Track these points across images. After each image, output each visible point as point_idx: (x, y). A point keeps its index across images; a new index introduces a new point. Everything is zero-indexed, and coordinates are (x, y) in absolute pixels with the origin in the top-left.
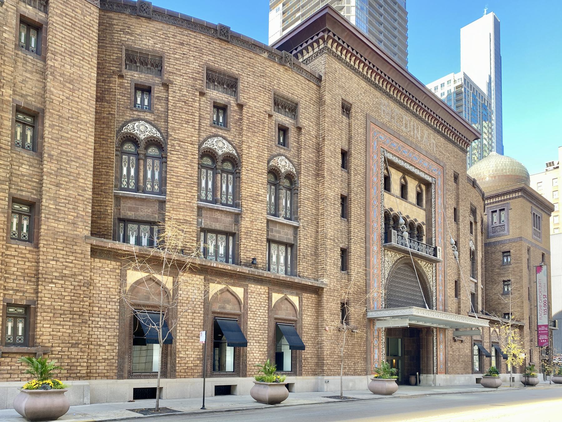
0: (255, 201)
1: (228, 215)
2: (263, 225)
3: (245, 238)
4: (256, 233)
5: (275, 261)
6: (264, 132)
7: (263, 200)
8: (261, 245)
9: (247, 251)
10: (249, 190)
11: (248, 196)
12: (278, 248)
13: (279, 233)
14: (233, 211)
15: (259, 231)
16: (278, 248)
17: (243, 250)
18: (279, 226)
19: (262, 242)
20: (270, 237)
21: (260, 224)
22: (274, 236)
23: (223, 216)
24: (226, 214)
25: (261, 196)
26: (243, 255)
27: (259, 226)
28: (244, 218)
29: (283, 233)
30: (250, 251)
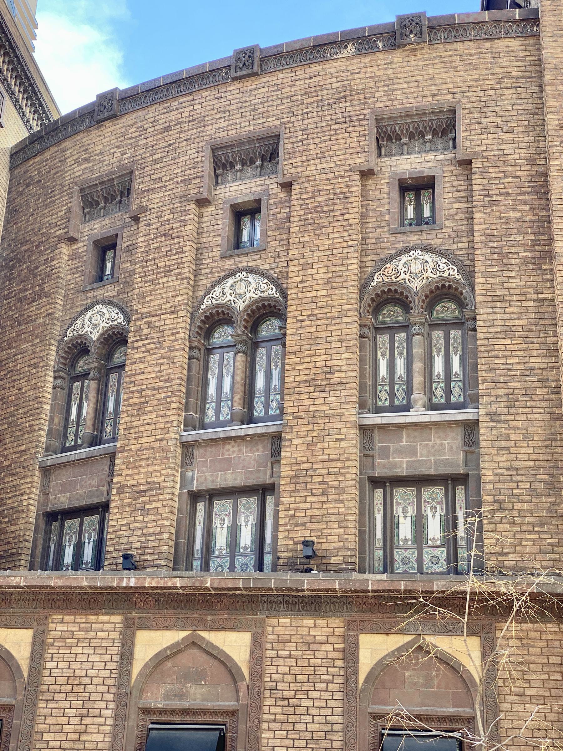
0: (322, 388)
1: (257, 444)
2: (343, 444)
3: (291, 491)
4: (325, 471)
5: (409, 536)
6: (346, 217)
7: (344, 380)
8: (339, 501)
9: (296, 525)
10: (304, 366)
11: (300, 382)
12: (419, 496)
13: (413, 452)
14: (264, 431)
15: (334, 464)
16: (419, 496)
17: (285, 525)
18: (408, 436)
19: (341, 490)
20: (378, 472)
21: (337, 444)
22: (395, 466)
23: (244, 449)
24: (251, 441)
25: (340, 371)
26: (287, 537)
27: (333, 451)
28: (290, 440)
29: (425, 452)
30: (304, 524)
